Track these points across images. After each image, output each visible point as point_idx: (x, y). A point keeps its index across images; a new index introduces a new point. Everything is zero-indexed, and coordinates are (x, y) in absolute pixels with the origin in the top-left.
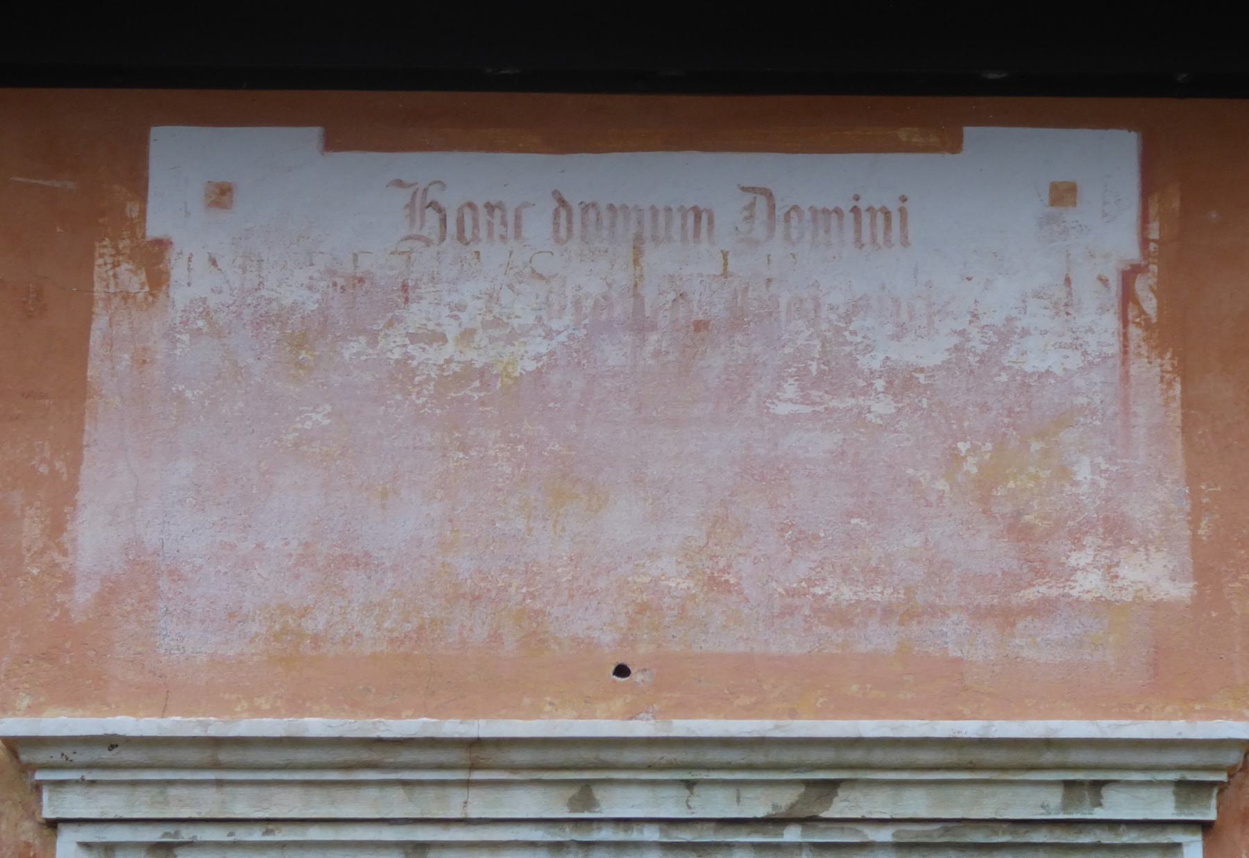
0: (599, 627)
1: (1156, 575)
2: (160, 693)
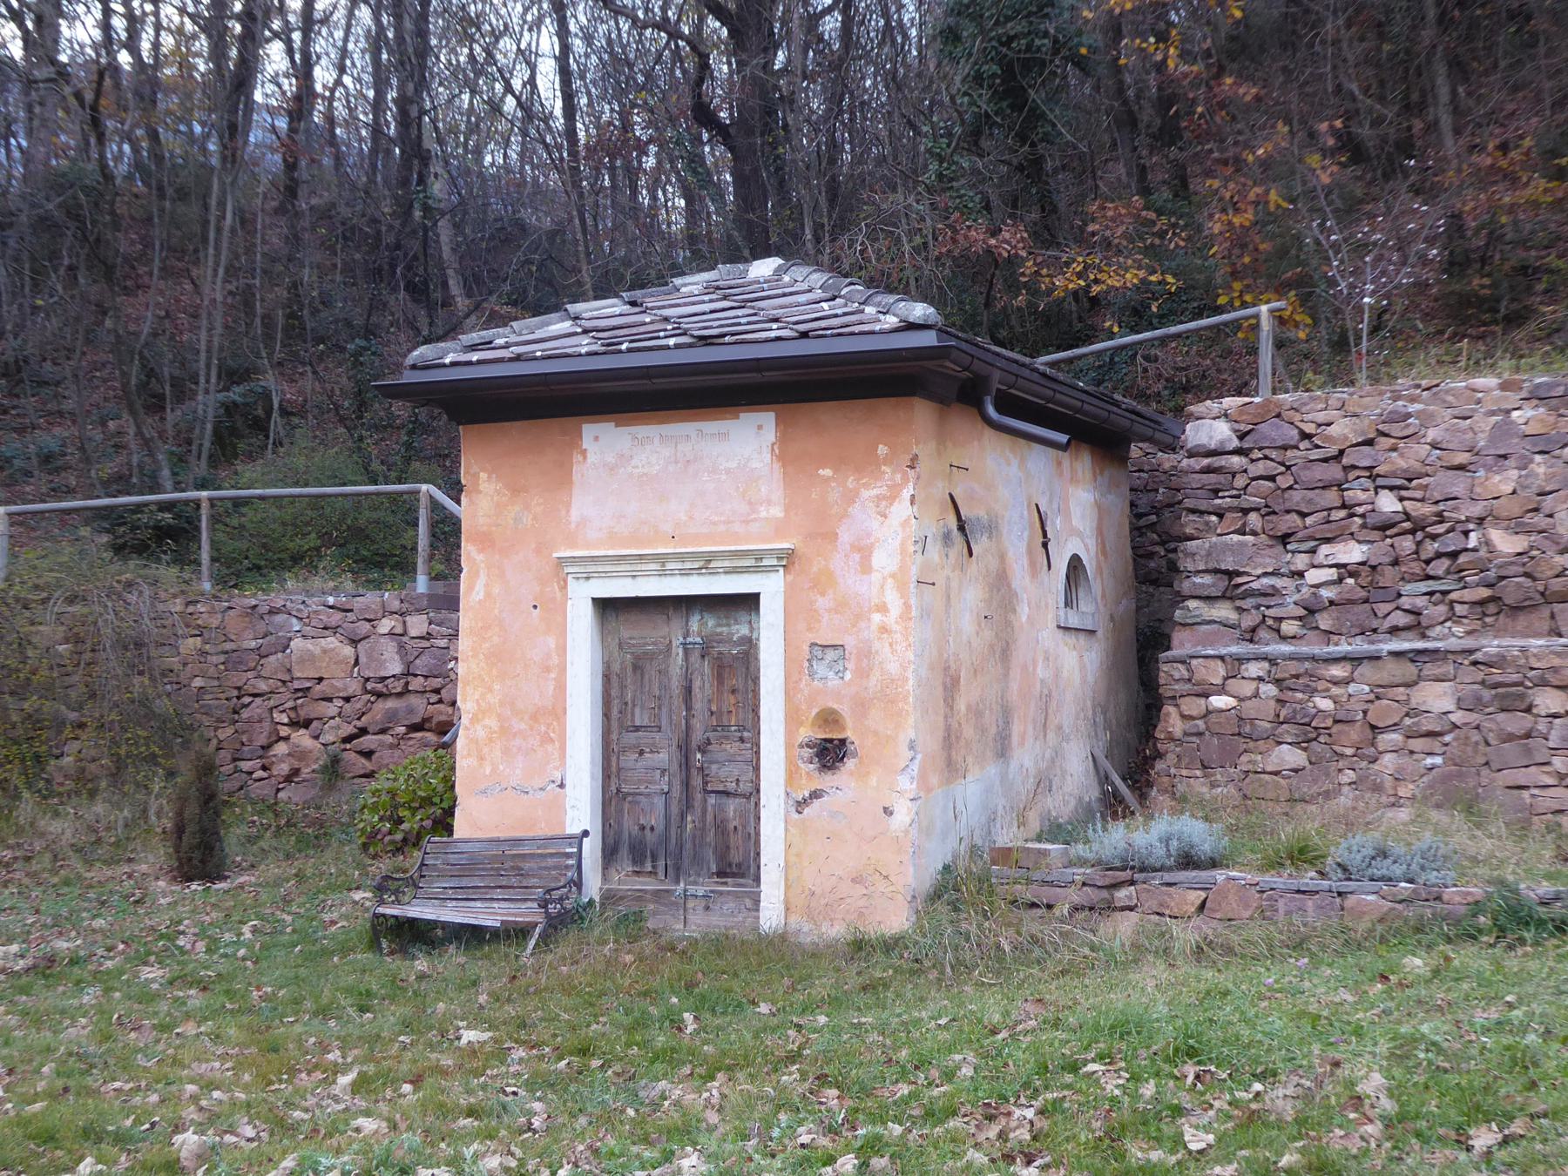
0: (668, 528)
1: (777, 512)
2: (588, 546)
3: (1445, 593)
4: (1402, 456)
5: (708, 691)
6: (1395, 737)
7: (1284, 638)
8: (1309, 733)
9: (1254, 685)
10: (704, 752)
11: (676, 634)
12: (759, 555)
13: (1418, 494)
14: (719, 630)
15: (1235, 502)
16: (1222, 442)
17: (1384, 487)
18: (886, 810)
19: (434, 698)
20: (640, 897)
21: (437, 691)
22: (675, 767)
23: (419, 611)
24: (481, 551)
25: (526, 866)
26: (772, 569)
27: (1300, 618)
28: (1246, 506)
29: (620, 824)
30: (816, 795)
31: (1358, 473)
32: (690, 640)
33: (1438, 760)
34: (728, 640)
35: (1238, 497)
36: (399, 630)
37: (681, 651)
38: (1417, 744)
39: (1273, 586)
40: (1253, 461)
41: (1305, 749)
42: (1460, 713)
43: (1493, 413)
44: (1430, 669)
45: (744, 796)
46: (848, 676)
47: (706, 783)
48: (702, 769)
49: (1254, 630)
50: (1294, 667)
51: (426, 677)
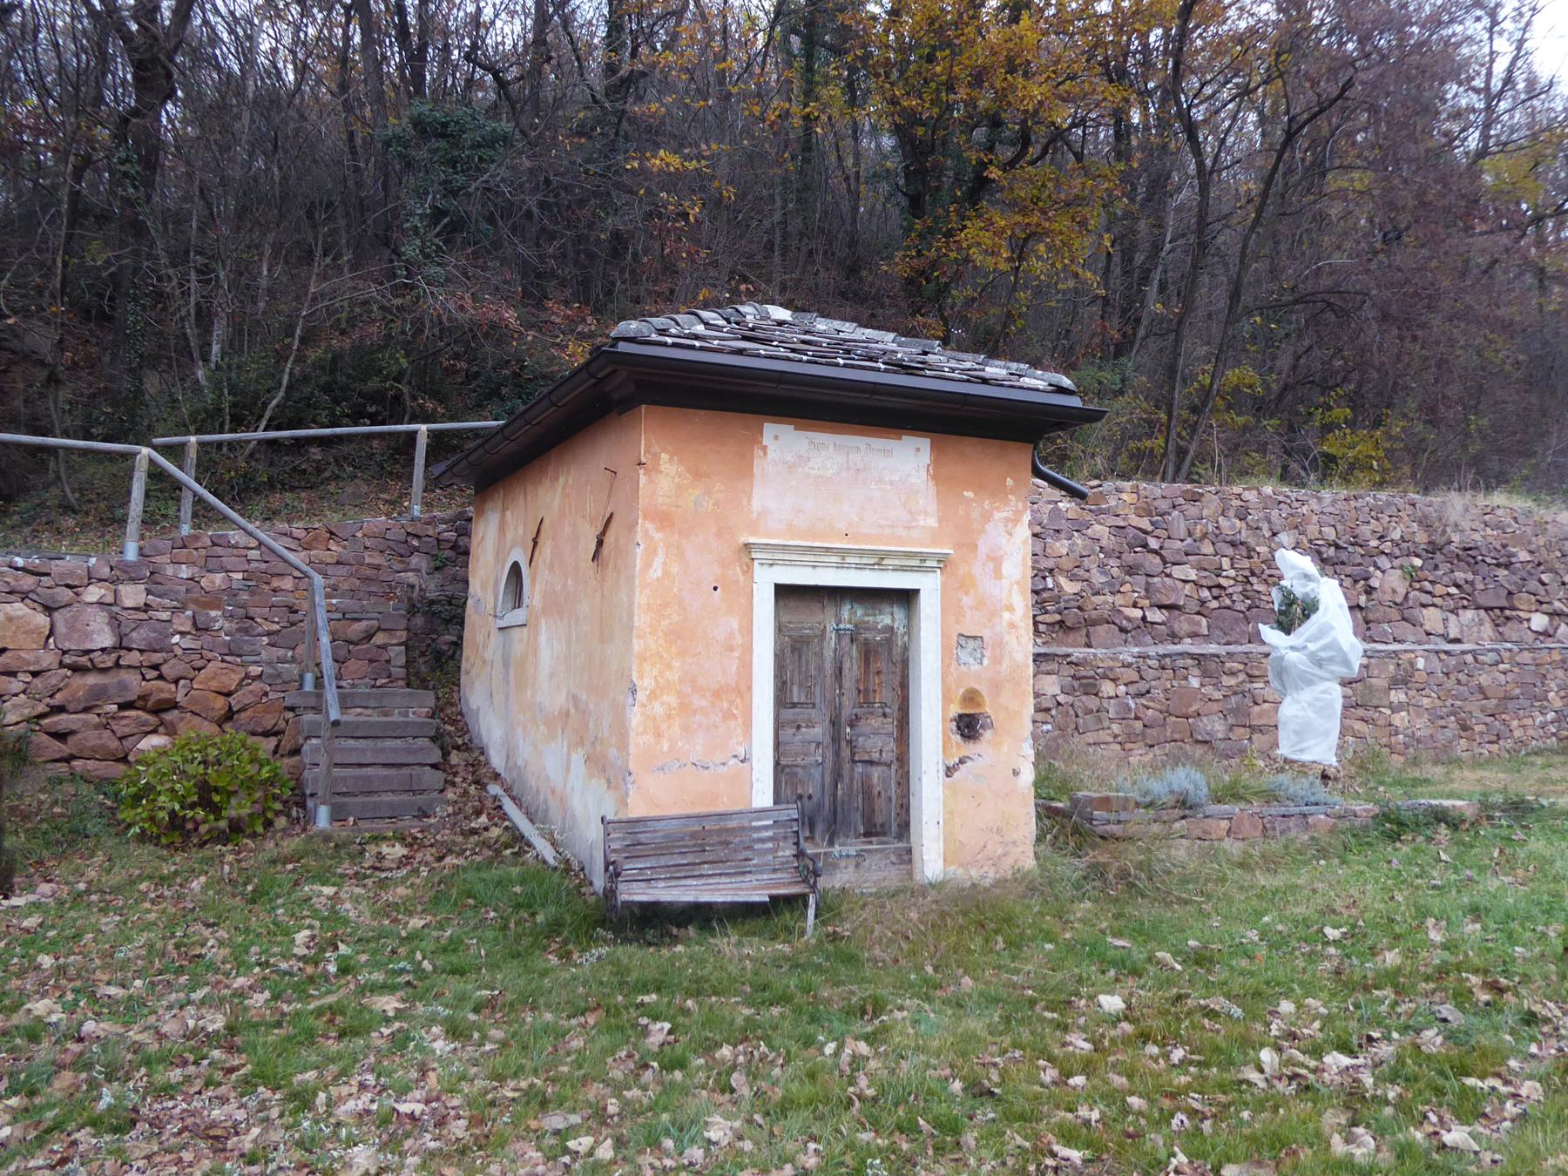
0: (842, 526)
1: (932, 522)
5: (855, 672)
10: (852, 726)
22: (828, 739)
24: (659, 529)
26: (932, 570)
30: (962, 761)
33: (1049, 727)
43: (1049, 502)
46: (986, 662)
47: (853, 754)
48: (850, 741)
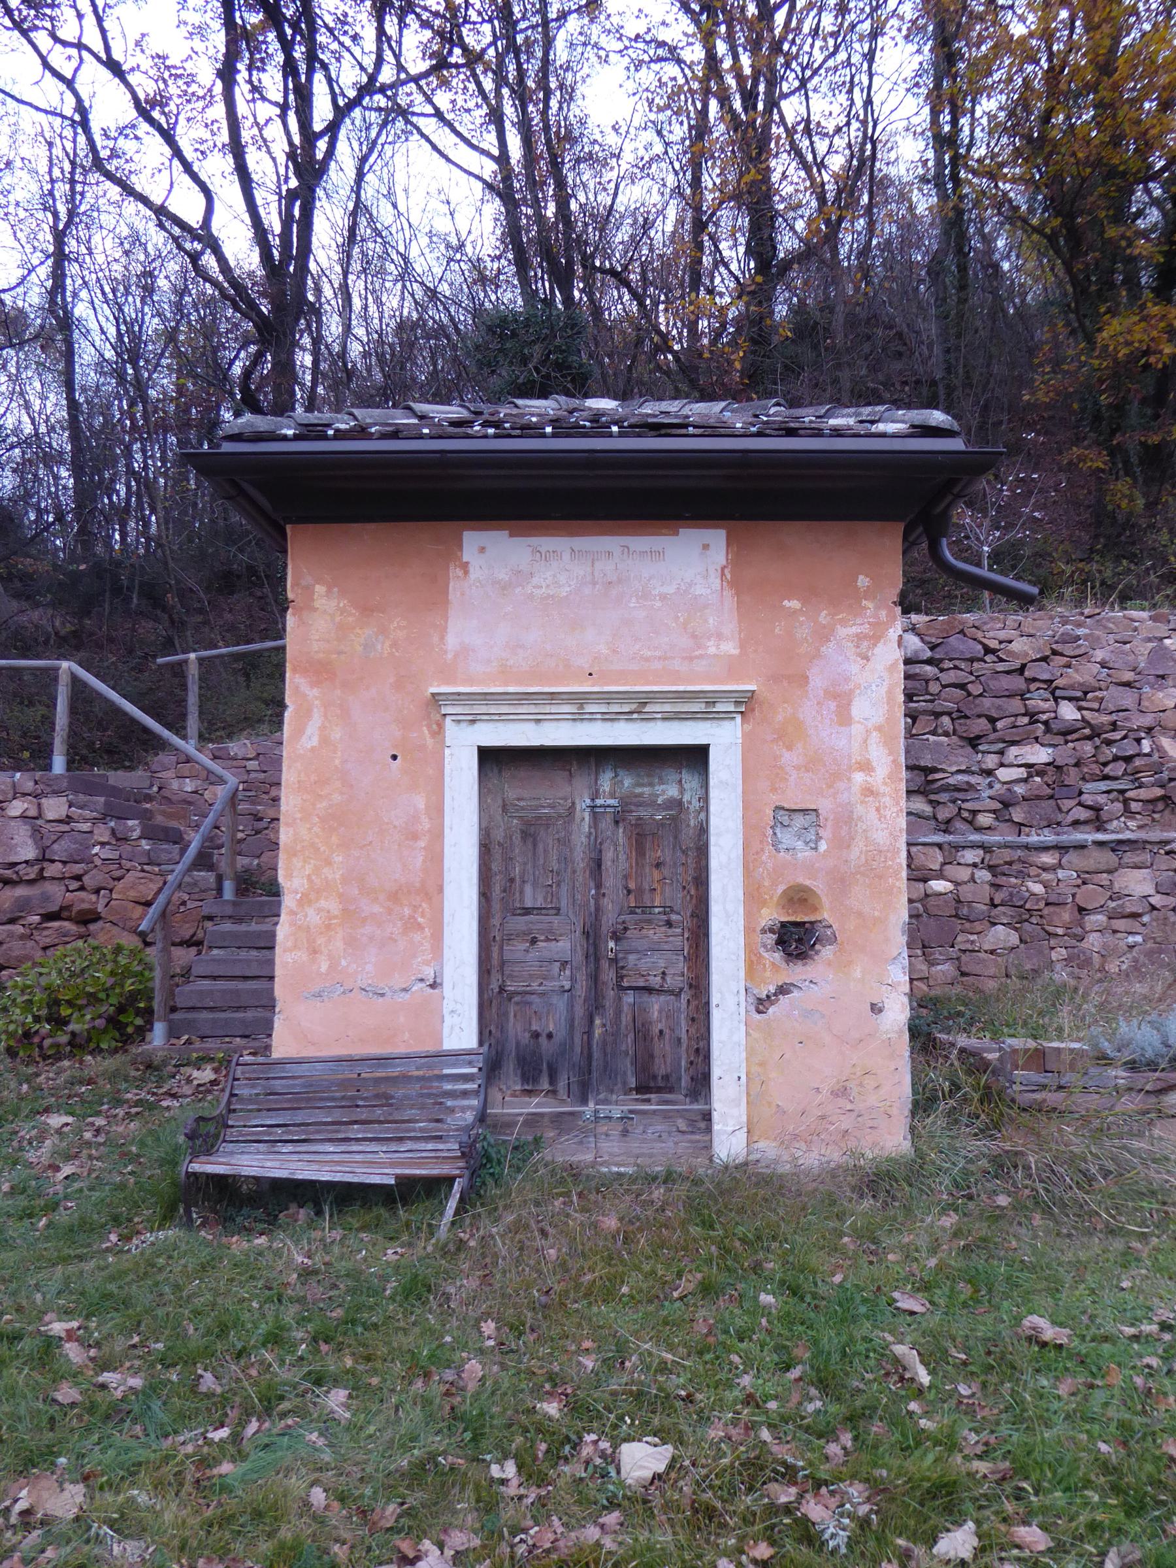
0: (584, 663)
1: (730, 648)
2: (470, 681)
3: (1122, 792)
4: (1077, 671)
5: (623, 864)
6: (1101, 918)
7: (979, 829)
8: (1022, 913)
9: (969, 870)
10: (616, 938)
11: (587, 798)
12: (711, 698)
13: (1096, 705)
14: (638, 790)
15: (930, 706)
16: (916, 652)
17: (1064, 698)
18: (873, 1006)
19: (74, 885)
20: (533, 1120)
21: (78, 878)
22: (579, 957)
23: (57, 793)
24: (313, 685)
25: (399, 1092)
26: (728, 716)
27: (994, 812)
28: (938, 709)
29: (502, 1029)
30: (783, 990)
31: (1038, 685)
32: (599, 802)
33: (1139, 939)
34: (652, 804)
35: (932, 701)
36: (33, 812)
37: (587, 815)
38: (1120, 924)
39: (968, 783)
40: (942, 670)
41: (1016, 929)
42: (1159, 896)
43: (1149, 640)
44: (1129, 858)
45: (671, 992)
46: (823, 846)
47: (621, 978)
48: (615, 961)
49: (949, 821)
50: (1007, 854)
51: (64, 863)
